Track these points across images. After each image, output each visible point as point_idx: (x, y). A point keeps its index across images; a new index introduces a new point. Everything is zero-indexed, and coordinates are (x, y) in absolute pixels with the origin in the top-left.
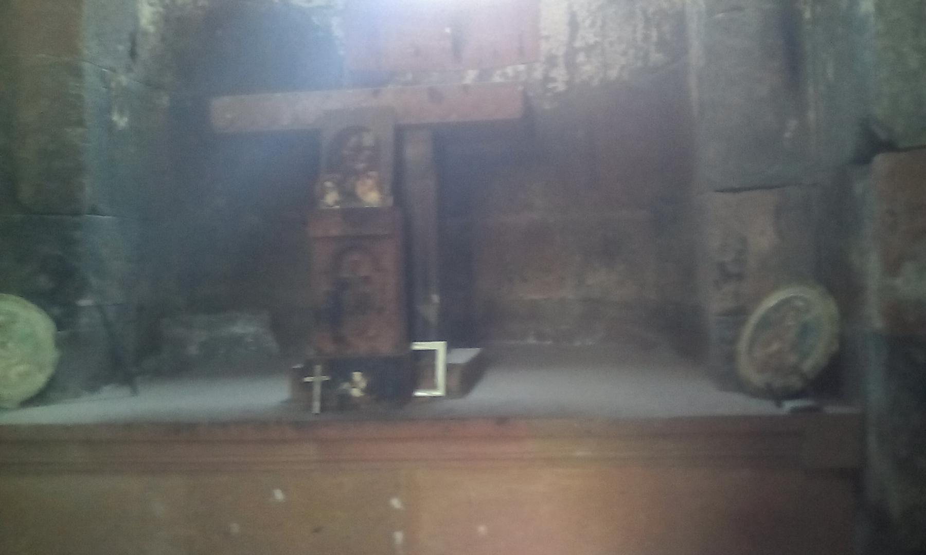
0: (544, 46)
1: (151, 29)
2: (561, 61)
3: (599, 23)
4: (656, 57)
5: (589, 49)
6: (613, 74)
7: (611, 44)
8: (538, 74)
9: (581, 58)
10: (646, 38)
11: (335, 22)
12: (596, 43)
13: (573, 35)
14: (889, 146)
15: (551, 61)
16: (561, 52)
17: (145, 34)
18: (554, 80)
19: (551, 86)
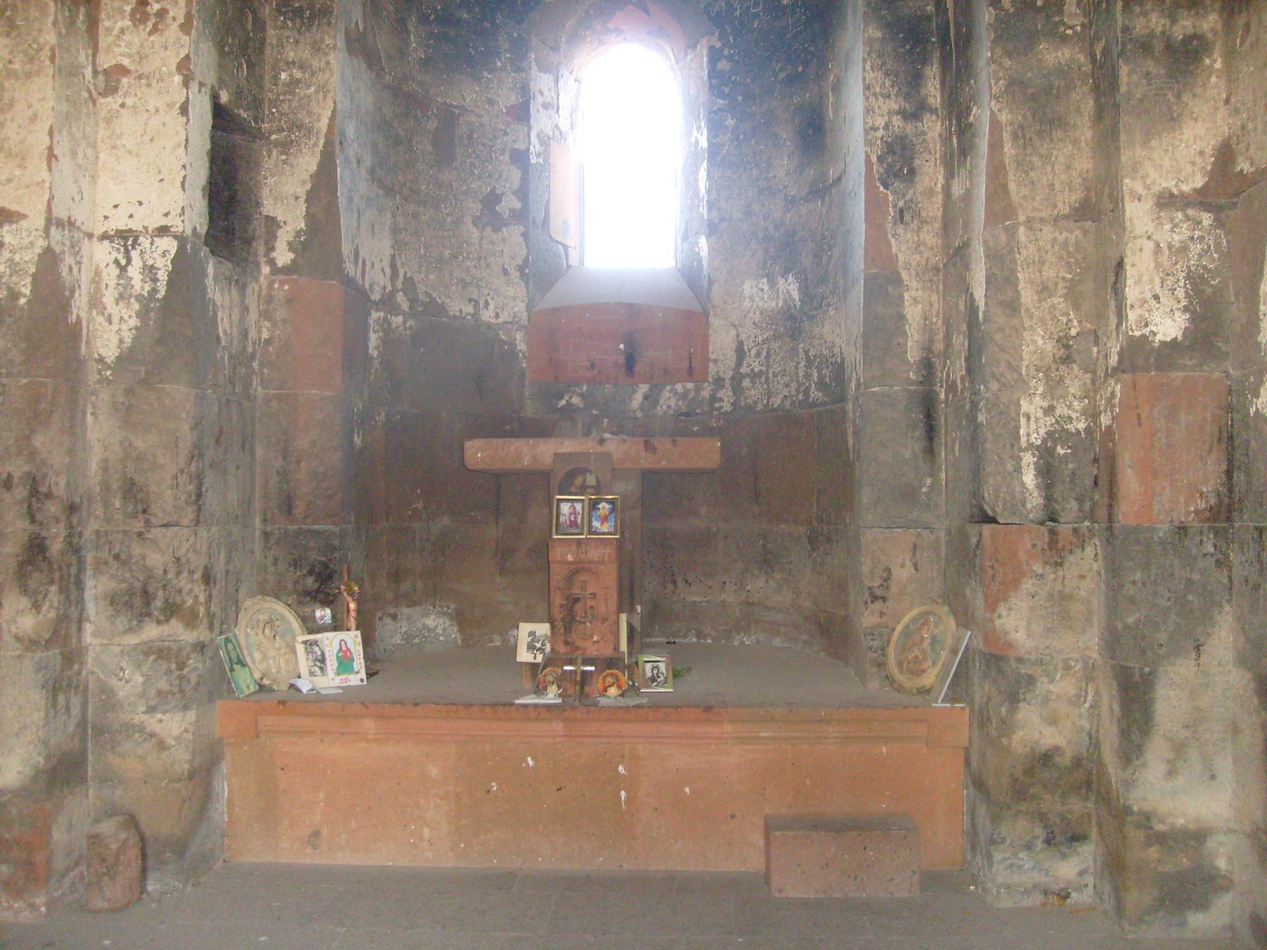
1: (375, 353)
2: (728, 382)
3: (764, 353)
4: (815, 394)
5: (755, 376)
6: (776, 401)
7: (775, 375)
8: (706, 393)
9: (746, 383)
11: (519, 336)
14: (994, 521)
15: (719, 382)
17: (372, 357)
18: (721, 400)
19: (717, 405)
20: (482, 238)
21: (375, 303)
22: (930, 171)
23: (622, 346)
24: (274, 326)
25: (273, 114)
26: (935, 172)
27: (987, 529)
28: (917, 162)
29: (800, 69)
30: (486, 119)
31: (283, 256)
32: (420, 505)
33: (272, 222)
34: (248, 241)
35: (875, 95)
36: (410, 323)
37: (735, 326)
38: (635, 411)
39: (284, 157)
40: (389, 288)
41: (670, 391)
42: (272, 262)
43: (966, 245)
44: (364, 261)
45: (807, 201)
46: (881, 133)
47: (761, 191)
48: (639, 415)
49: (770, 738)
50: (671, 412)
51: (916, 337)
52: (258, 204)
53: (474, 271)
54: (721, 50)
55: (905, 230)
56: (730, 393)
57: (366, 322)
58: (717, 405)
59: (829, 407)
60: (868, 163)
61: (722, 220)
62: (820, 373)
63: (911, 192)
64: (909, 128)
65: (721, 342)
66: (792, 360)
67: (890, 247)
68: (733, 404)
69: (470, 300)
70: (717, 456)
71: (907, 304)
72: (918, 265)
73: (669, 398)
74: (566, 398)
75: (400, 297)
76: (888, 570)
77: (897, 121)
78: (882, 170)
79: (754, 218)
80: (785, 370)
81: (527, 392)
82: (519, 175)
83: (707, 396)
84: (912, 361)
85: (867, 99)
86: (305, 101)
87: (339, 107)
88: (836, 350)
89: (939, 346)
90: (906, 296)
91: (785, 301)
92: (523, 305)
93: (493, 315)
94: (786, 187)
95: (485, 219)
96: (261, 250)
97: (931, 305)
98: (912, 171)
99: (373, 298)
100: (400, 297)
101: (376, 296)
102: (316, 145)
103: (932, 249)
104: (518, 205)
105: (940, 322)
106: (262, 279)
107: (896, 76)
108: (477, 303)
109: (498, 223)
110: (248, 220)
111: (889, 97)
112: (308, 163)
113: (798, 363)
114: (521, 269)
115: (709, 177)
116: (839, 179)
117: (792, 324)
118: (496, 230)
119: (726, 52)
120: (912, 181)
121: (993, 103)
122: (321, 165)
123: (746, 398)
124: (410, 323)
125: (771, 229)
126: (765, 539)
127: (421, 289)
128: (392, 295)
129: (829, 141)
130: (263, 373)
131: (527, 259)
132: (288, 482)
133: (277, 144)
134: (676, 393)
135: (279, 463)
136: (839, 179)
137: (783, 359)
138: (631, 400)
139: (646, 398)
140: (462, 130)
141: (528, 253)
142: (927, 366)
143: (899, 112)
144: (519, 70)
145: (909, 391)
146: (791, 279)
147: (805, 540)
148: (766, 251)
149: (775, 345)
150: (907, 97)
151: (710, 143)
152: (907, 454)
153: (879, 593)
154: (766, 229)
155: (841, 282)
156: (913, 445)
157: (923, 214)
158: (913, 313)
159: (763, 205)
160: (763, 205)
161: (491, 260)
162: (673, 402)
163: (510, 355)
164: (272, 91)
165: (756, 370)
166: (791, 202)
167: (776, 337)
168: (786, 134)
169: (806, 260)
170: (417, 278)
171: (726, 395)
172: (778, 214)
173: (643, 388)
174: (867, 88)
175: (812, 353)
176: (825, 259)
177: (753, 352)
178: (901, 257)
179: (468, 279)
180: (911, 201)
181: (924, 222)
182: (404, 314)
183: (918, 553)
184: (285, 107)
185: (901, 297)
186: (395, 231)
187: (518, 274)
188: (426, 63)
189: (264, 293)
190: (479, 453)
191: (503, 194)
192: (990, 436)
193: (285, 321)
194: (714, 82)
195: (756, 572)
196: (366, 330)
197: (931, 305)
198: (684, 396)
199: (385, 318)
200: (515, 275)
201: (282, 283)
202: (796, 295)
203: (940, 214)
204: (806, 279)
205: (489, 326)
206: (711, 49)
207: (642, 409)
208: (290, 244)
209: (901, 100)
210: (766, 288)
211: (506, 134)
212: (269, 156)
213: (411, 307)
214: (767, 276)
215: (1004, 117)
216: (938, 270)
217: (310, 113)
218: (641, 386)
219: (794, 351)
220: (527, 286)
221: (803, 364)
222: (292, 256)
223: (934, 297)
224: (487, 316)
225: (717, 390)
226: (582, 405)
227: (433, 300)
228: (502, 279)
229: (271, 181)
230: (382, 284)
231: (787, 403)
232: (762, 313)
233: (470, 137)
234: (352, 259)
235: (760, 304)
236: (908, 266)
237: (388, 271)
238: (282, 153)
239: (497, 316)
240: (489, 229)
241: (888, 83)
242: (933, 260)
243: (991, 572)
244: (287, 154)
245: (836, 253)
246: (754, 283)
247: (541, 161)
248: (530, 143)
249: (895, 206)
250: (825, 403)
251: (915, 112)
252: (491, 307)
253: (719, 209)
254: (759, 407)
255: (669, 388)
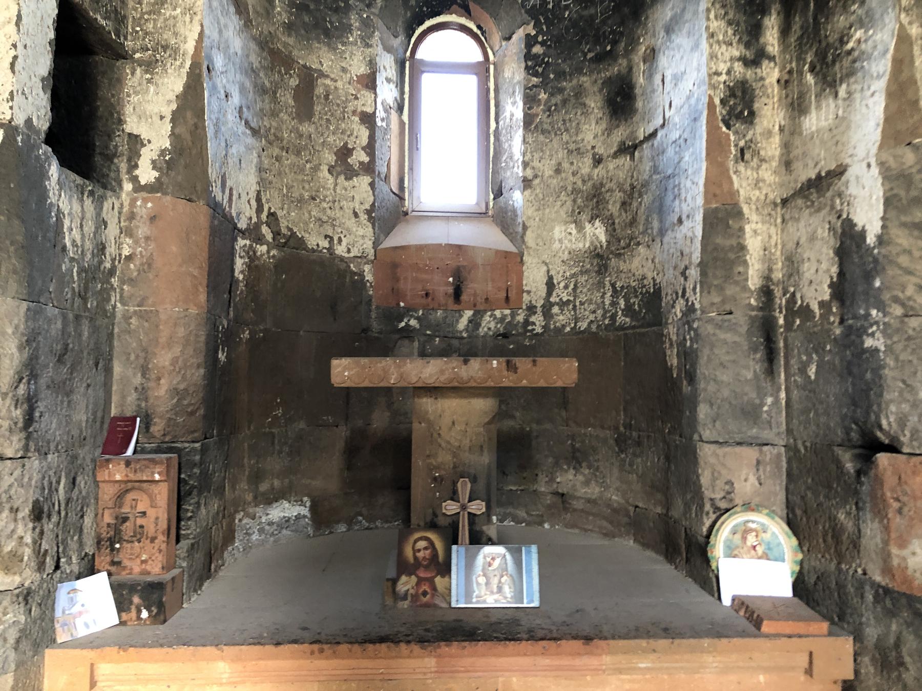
0: (526, 298)
1: (241, 277)
2: (539, 310)
3: (572, 286)
4: (621, 319)
5: (563, 304)
6: (583, 325)
7: (582, 304)
8: (520, 318)
9: (556, 310)
10: (614, 304)
11: (367, 268)
12: (568, 300)
13: (549, 293)
14: (893, 448)
15: (531, 309)
16: (539, 305)
17: (238, 281)
19: (530, 328)
20: (336, 185)
21: (240, 231)
22: (769, 113)
23: (451, 279)
24: (136, 242)
25: (137, 32)
26: (772, 115)
27: (883, 459)
28: (756, 106)
29: (609, 48)
30: (340, 84)
31: (146, 174)
32: (280, 412)
33: (136, 141)
34: (110, 158)
35: (718, 42)
36: (274, 252)
37: (546, 264)
38: (461, 332)
39: (148, 76)
40: (255, 220)
41: (490, 316)
42: (135, 180)
43: (840, 172)
44: (231, 189)
45: (615, 155)
46: (724, 77)
47: (570, 152)
48: (465, 335)
49: (647, 669)
50: (491, 333)
51: (757, 266)
52: (120, 122)
53: (329, 211)
54: (536, 36)
55: (746, 168)
56: (542, 318)
57: (233, 248)
58: (530, 328)
59: (638, 330)
60: (711, 105)
61: (536, 176)
62: (627, 301)
63: (751, 132)
64: (749, 74)
65: (534, 278)
66: (598, 291)
67: (732, 183)
68: (543, 327)
69: (326, 237)
70: (575, 376)
71: (747, 235)
72: (758, 199)
73: (489, 322)
74: (406, 320)
75: (265, 229)
76: (730, 483)
77: (738, 67)
78: (724, 112)
79: (563, 175)
80: (591, 300)
81: (373, 315)
82: (368, 134)
83: (522, 320)
84: (753, 288)
85: (711, 46)
86: (171, 22)
87: (207, 32)
88: (648, 282)
89: (778, 275)
90: (747, 228)
91: (592, 243)
92: (370, 243)
93: (346, 250)
94: (593, 147)
95: (339, 169)
96: (123, 167)
97: (770, 237)
98: (752, 114)
99: (239, 226)
100: (265, 229)
101: (242, 224)
102: (182, 66)
103: (770, 185)
104: (366, 159)
105: (778, 253)
106: (124, 196)
107: (738, 24)
108: (332, 238)
109: (350, 173)
110: (110, 136)
111: (731, 44)
112: (173, 83)
113: (604, 293)
114: (369, 212)
115: (524, 141)
116: (654, 134)
117: (600, 261)
118: (348, 178)
119: (540, 39)
120: (752, 123)
121: (903, 16)
122: (188, 87)
123: (555, 323)
124: (274, 252)
125: (580, 183)
126: (573, 440)
127: (283, 224)
128: (258, 226)
129: (639, 104)
130: (122, 289)
131: (373, 205)
132: (146, 400)
133: (140, 63)
134: (495, 318)
135: (138, 380)
136: (654, 134)
137: (589, 290)
138: (457, 321)
139: (470, 321)
140: (319, 91)
141: (375, 200)
142: (766, 292)
143: (739, 59)
144: (368, 46)
145: (751, 317)
146: (597, 223)
147: (612, 442)
148: (574, 201)
149: (582, 279)
150: (747, 45)
151: (526, 115)
152: (750, 375)
153: (723, 505)
154: (575, 183)
155: (656, 224)
156: (752, 367)
157: (762, 153)
158: (753, 245)
159: (572, 163)
160: (572, 163)
161: (344, 203)
162: (492, 325)
163: (360, 283)
164: (135, 9)
165: (565, 299)
166: (598, 161)
167: (582, 273)
168: (595, 103)
169: (613, 208)
170: (280, 213)
171: (538, 320)
172: (585, 170)
173: (469, 313)
174: (712, 35)
175: (619, 284)
176: (635, 204)
177: (562, 285)
178: (742, 192)
179: (325, 218)
180: (751, 141)
181: (763, 160)
182: (268, 244)
183: (761, 468)
184: (150, 26)
185: (741, 229)
186: (260, 170)
187: (366, 216)
188: (289, 27)
189: (125, 210)
190: (345, 371)
191: (354, 149)
192: (890, 362)
193: (147, 238)
194: (530, 63)
195: (565, 467)
196: (232, 255)
197: (770, 237)
198: (502, 319)
199: (251, 246)
200: (363, 217)
201: (145, 201)
202: (603, 238)
203: (777, 153)
204: (614, 223)
205: (342, 259)
206: (528, 35)
207: (466, 330)
208: (153, 162)
209: (742, 47)
210: (574, 232)
211: (356, 98)
212: (133, 74)
213: (274, 239)
214: (575, 222)
215: (914, 31)
216: (775, 205)
217: (176, 34)
218: (466, 312)
219: (601, 284)
220: (374, 228)
221: (609, 294)
222: (156, 174)
223: (773, 230)
224: (340, 250)
225: (530, 316)
226: (418, 326)
227: (293, 234)
228: (353, 220)
229: (134, 99)
230: (248, 214)
231: (594, 327)
232: (570, 253)
233: (327, 97)
234: (219, 183)
235: (569, 246)
236: (748, 201)
237: (254, 204)
238: (147, 72)
239: (349, 251)
240: (342, 177)
241: (730, 32)
242: (771, 196)
243: (896, 505)
244: (152, 74)
245: (647, 199)
246: (563, 228)
247: (384, 124)
248: (376, 109)
249: (736, 146)
250: (634, 327)
251: (756, 58)
252: (344, 243)
253: (533, 168)
254: (568, 329)
255: (489, 313)
